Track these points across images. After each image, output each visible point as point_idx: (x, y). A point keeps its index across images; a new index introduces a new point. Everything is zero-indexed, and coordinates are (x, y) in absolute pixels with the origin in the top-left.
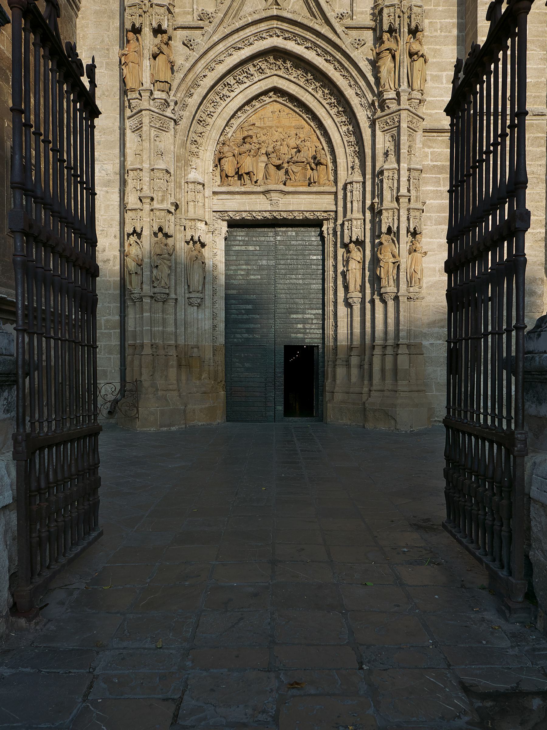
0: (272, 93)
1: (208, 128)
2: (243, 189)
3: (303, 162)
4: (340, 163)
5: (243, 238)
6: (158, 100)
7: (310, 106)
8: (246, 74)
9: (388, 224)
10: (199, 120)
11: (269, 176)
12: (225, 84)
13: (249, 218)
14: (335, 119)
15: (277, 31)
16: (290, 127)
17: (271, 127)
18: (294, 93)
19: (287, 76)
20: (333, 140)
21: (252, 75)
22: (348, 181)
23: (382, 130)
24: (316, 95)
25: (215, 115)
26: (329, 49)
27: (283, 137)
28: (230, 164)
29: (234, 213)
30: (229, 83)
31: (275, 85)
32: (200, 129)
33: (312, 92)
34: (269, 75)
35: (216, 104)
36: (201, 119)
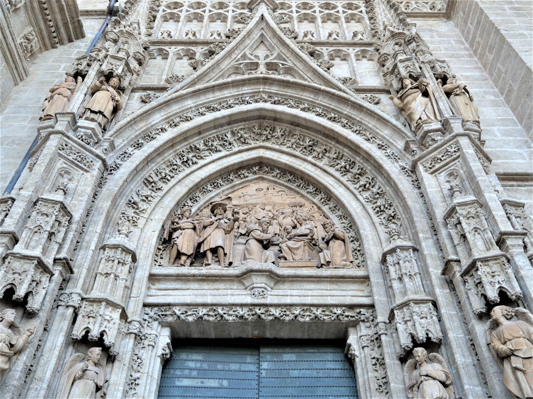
0: (257, 168)
1: (160, 194)
2: (204, 270)
3: (306, 235)
4: (366, 236)
5: (198, 365)
6: (83, 130)
8: (221, 143)
9: (497, 286)
10: (147, 179)
11: (250, 254)
12: (191, 147)
13: (211, 319)
15: (264, 96)
16: (282, 204)
17: (255, 205)
19: (277, 147)
21: (230, 144)
23: (432, 170)
25: (173, 181)
26: (333, 105)
28: (186, 237)
29: (184, 309)
30: (198, 146)
32: (146, 191)
33: (313, 161)
34: (253, 145)
35: (175, 167)
36: (150, 179)
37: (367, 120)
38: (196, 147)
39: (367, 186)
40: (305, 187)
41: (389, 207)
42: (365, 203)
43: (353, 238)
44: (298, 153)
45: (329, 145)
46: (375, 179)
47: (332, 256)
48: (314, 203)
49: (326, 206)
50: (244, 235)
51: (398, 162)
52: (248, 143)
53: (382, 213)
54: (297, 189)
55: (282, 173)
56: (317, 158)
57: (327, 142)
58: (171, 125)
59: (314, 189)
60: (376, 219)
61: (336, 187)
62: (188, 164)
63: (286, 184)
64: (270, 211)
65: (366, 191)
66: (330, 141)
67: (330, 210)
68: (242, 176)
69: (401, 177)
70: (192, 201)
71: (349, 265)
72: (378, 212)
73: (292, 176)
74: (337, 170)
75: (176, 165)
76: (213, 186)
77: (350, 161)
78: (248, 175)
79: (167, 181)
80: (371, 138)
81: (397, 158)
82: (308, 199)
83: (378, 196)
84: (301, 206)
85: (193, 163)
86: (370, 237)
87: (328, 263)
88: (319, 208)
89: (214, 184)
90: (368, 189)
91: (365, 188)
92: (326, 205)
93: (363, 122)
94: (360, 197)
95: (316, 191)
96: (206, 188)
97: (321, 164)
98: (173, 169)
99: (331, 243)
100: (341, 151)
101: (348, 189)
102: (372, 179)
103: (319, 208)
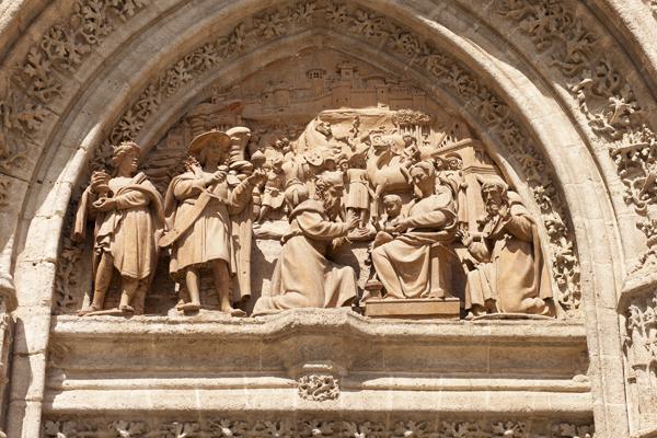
27: (350, 154)
35: (91, 26)
36: (30, 70)
40: (438, 71)
41: (650, 157)
42: (592, 135)
49: (491, 129)
53: (632, 169)
55: (376, 25)
59: (461, 80)
62: (125, 13)
64: (344, 140)
68: (269, 34)
70: (140, 114)
71: (543, 308)
73: (404, 38)
75: (93, 20)
76: (191, 67)
79: (72, 69)
86: (598, 234)
92: (494, 124)
95: (467, 84)
98: (87, 31)
99: (500, 244)
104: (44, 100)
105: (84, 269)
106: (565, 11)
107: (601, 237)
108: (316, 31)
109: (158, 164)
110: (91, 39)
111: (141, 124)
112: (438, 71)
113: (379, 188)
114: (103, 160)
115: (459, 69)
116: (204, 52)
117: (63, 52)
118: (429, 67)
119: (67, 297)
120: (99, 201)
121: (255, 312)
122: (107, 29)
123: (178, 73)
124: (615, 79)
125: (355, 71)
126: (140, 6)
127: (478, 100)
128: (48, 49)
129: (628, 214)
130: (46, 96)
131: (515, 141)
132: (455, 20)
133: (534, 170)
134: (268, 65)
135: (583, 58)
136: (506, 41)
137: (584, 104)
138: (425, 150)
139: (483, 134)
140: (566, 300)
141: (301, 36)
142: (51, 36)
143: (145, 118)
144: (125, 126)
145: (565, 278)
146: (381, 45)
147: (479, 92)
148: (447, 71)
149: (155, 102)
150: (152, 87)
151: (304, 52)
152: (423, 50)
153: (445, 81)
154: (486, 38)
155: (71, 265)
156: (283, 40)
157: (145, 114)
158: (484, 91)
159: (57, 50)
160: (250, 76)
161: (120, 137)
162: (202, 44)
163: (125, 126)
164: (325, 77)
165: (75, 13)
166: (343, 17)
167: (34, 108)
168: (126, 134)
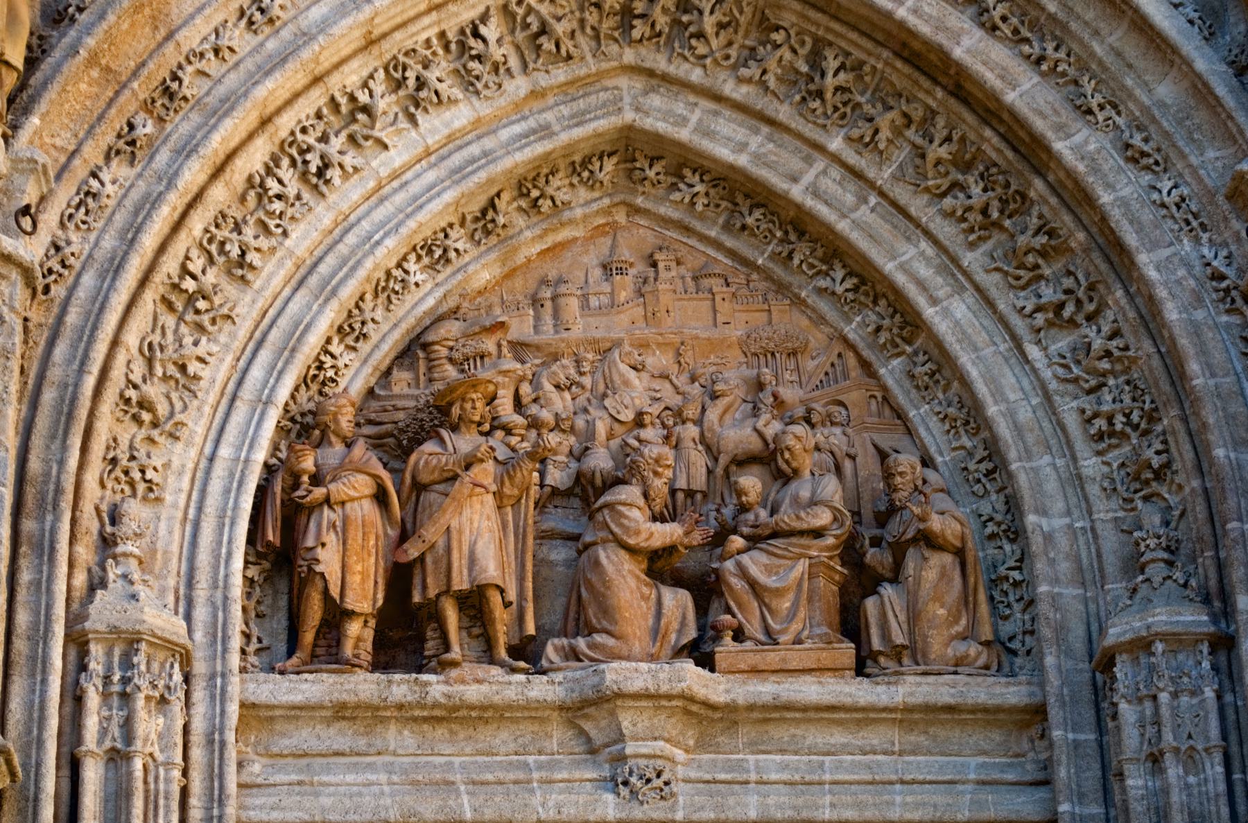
7: (843, 226)
14: (994, 293)
18: (742, 160)
19: (696, 75)
20: (992, 410)
22: (1116, 632)
24: (871, 173)
30: (363, 98)
31: (629, 116)
33: (852, 158)
35: (277, 206)
36: (189, 285)
37: (1089, 15)
38: (352, 98)
39: (1067, 312)
40: (812, 266)
42: (1053, 385)
43: (999, 524)
44: (784, 112)
45: (921, 95)
46: (1101, 287)
47: (914, 616)
48: (845, 340)
49: (895, 362)
50: (568, 493)
51: (1197, 241)
52: (569, 57)
53: (1114, 441)
54: (778, 271)
55: (712, 192)
56: (867, 144)
57: (916, 82)
58: (251, 23)
59: (849, 284)
60: (1091, 465)
61: (941, 294)
63: (729, 242)
65: (1061, 327)
66: (926, 84)
67: (907, 384)
68: (546, 205)
69: (1200, 315)
70: (350, 341)
72: (1100, 436)
73: (757, 214)
74: (949, 215)
75: (279, 197)
77: (1007, 185)
78: (566, 198)
80: (1102, 108)
81: (1195, 224)
82: (821, 320)
83: (1105, 365)
84: (793, 353)
85: (346, 176)
87: (897, 653)
88: (865, 365)
89: (430, 252)
90: (1072, 323)
91: (1057, 318)
92: (898, 355)
93: (1073, 26)
94: (1033, 352)
95: (855, 289)
96: (398, 273)
97: (883, 175)
98: (271, 214)
100: (972, 136)
101: (990, 304)
102: (1091, 287)
103: (865, 365)
104: (210, 328)
105: (276, 592)
106: (1013, 188)
107: (1067, 549)
108: (617, 199)
109: (384, 417)
110: (278, 226)
111: (353, 355)
112: (812, 266)
113: (723, 460)
114: (299, 418)
115: (844, 266)
116: (446, 236)
117: (235, 252)
118: (796, 262)
119: (254, 640)
120: (300, 493)
121: (544, 663)
122: (296, 211)
123: (406, 272)
124: (1091, 300)
125: (679, 263)
126: (351, 170)
127: (874, 317)
128: (213, 248)
129: (1106, 510)
130: (213, 321)
131: (931, 384)
132: (840, 191)
133: (962, 432)
134: (542, 253)
135: (1040, 261)
136: (918, 225)
137: (1042, 333)
138: (789, 394)
139: (882, 371)
140: (1011, 639)
141: (595, 207)
142: (217, 226)
143: (358, 345)
144: (328, 360)
145: (1009, 606)
146: (721, 221)
147: (875, 302)
148: (824, 268)
149: (373, 320)
150: (368, 297)
151: (599, 231)
152: (786, 233)
153: (823, 283)
154: (887, 221)
155: (258, 589)
156: (567, 215)
157: (357, 339)
158: (883, 302)
159: (228, 247)
160: (514, 270)
161: (321, 378)
162: (443, 224)
163: (328, 360)
164: (632, 271)
165: (253, 187)
166: (661, 177)
167: (196, 344)
168: (330, 373)
